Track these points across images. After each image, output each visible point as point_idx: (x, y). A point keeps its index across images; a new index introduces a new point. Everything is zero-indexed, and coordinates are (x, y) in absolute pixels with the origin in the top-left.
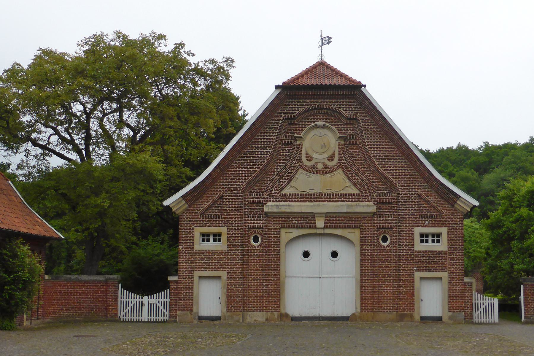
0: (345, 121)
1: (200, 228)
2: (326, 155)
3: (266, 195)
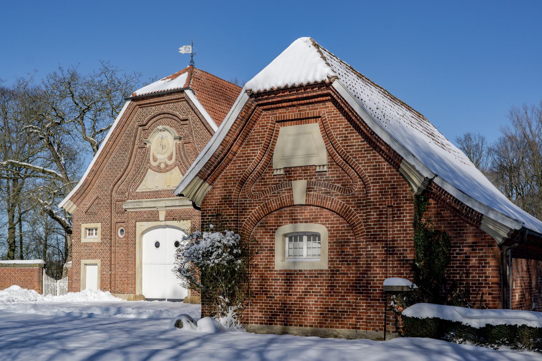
0: (182, 123)
1: (84, 224)
2: (167, 155)
3: (127, 194)
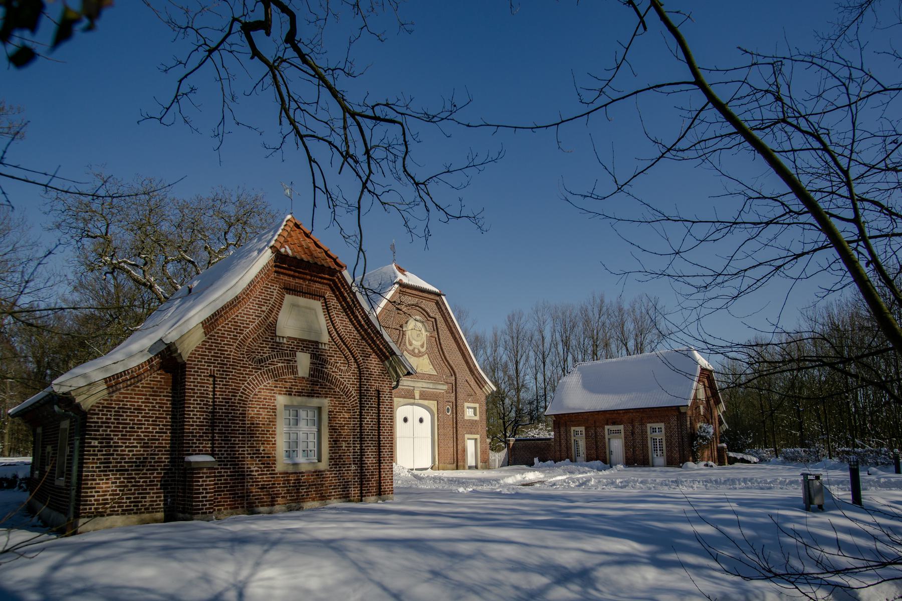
0: (429, 318)
